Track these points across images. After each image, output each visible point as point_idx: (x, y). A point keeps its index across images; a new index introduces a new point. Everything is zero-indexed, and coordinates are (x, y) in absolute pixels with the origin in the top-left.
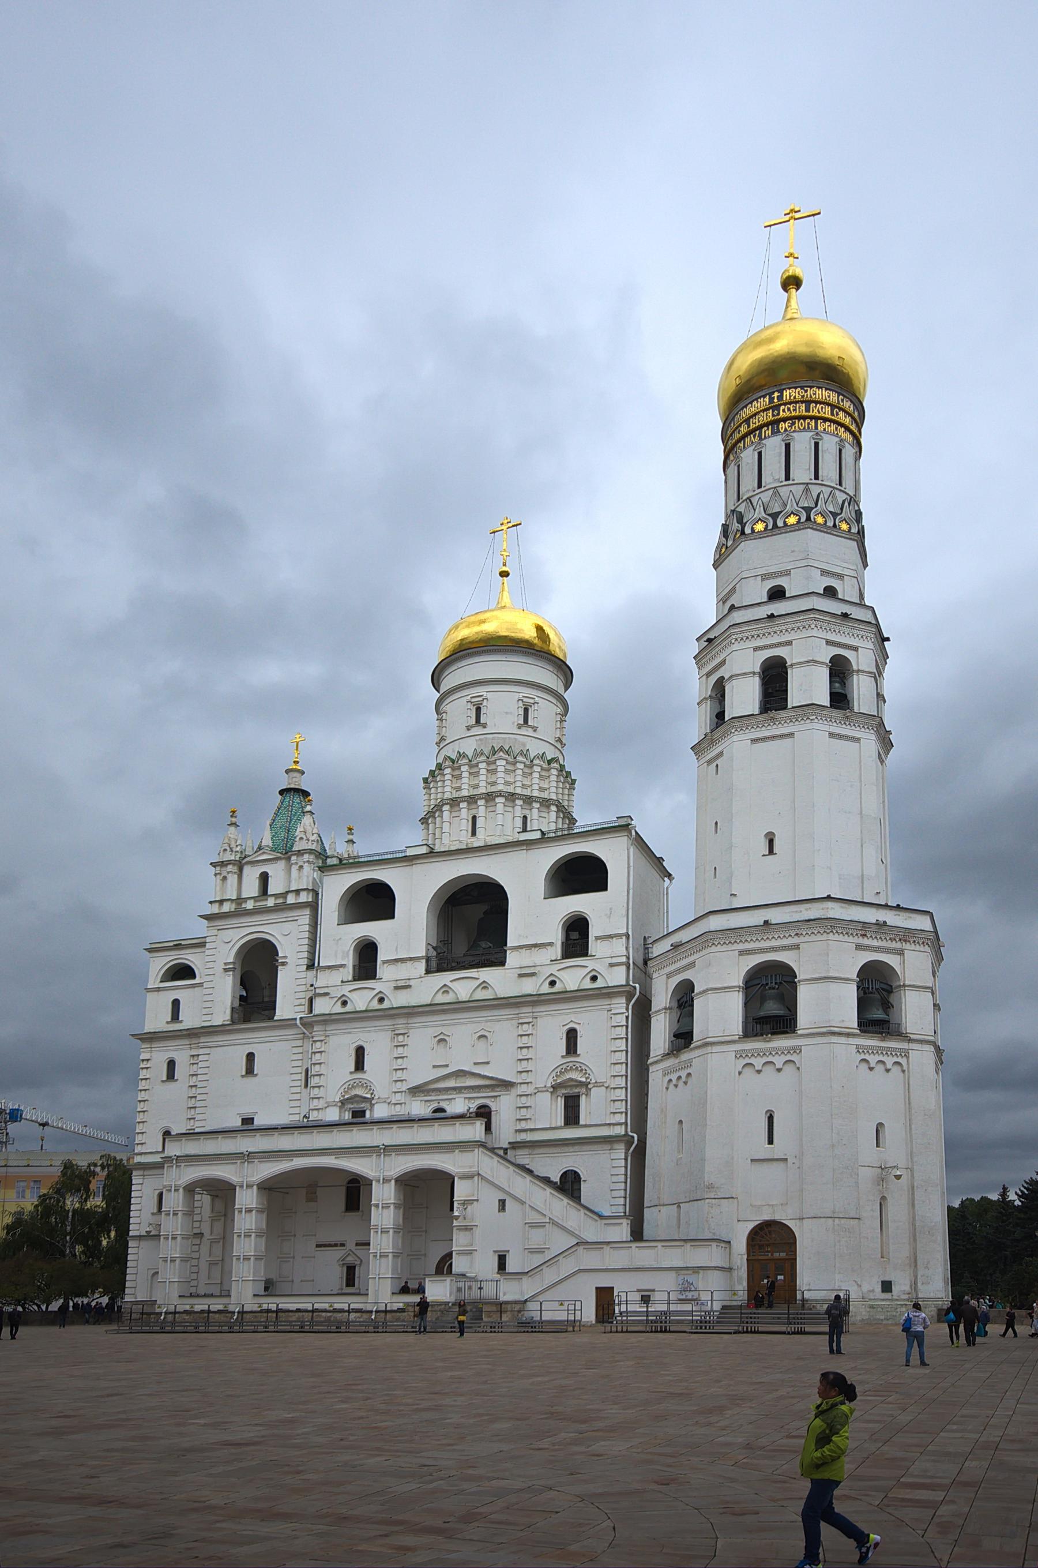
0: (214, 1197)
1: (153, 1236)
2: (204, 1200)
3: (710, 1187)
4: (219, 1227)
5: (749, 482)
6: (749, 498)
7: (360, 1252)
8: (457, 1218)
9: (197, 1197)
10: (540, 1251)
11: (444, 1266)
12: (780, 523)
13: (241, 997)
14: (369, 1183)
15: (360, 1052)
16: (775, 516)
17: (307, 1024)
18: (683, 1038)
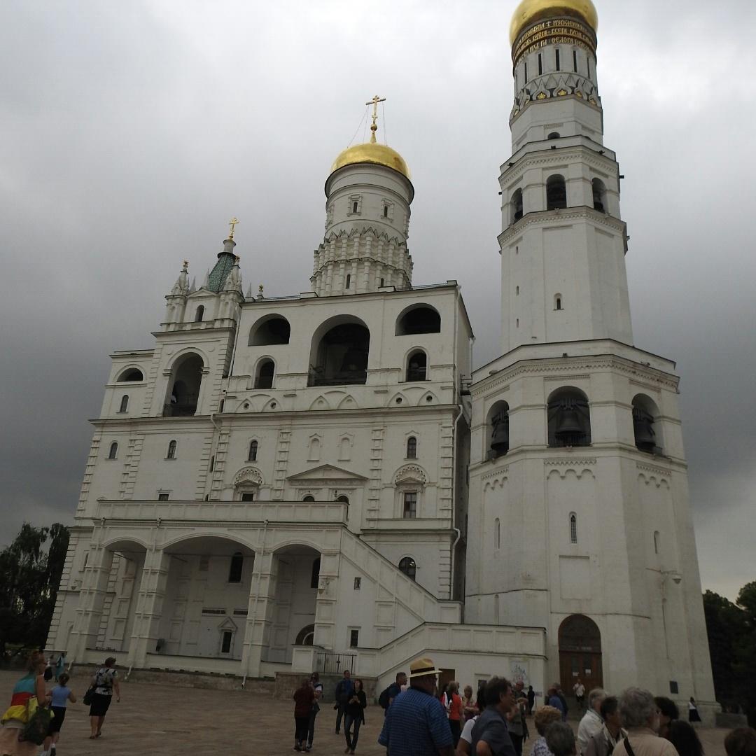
0: (129, 560)
1: (74, 592)
2: (120, 562)
3: (528, 579)
4: (129, 587)
5: (533, 72)
6: (534, 80)
7: (238, 620)
8: (321, 591)
9: (115, 560)
10: (386, 629)
11: (306, 637)
12: (555, 94)
13: (172, 401)
14: (251, 554)
15: (254, 445)
16: (552, 90)
17: (219, 418)
18: (499, 448)
